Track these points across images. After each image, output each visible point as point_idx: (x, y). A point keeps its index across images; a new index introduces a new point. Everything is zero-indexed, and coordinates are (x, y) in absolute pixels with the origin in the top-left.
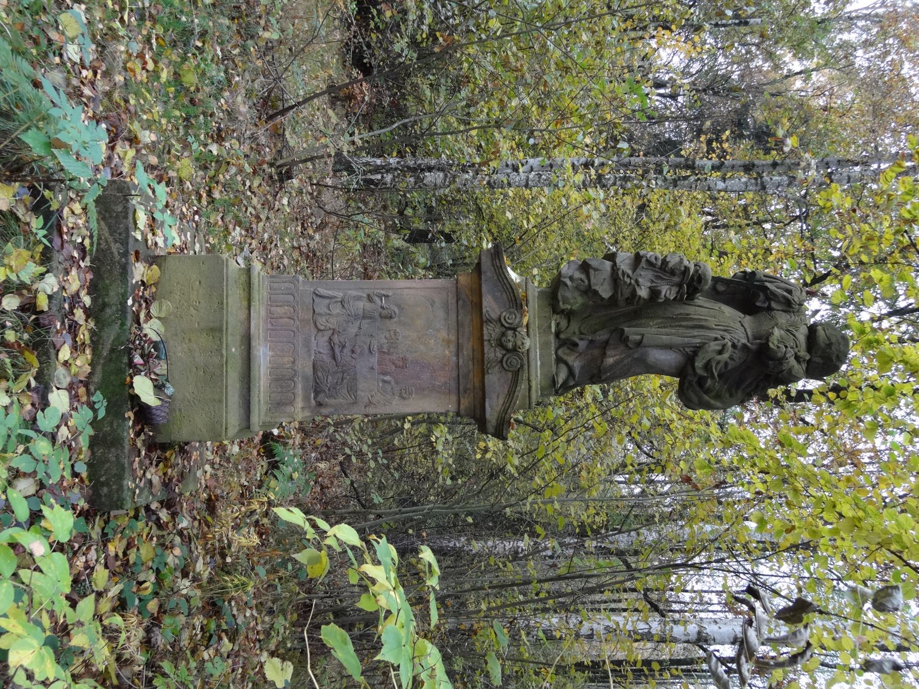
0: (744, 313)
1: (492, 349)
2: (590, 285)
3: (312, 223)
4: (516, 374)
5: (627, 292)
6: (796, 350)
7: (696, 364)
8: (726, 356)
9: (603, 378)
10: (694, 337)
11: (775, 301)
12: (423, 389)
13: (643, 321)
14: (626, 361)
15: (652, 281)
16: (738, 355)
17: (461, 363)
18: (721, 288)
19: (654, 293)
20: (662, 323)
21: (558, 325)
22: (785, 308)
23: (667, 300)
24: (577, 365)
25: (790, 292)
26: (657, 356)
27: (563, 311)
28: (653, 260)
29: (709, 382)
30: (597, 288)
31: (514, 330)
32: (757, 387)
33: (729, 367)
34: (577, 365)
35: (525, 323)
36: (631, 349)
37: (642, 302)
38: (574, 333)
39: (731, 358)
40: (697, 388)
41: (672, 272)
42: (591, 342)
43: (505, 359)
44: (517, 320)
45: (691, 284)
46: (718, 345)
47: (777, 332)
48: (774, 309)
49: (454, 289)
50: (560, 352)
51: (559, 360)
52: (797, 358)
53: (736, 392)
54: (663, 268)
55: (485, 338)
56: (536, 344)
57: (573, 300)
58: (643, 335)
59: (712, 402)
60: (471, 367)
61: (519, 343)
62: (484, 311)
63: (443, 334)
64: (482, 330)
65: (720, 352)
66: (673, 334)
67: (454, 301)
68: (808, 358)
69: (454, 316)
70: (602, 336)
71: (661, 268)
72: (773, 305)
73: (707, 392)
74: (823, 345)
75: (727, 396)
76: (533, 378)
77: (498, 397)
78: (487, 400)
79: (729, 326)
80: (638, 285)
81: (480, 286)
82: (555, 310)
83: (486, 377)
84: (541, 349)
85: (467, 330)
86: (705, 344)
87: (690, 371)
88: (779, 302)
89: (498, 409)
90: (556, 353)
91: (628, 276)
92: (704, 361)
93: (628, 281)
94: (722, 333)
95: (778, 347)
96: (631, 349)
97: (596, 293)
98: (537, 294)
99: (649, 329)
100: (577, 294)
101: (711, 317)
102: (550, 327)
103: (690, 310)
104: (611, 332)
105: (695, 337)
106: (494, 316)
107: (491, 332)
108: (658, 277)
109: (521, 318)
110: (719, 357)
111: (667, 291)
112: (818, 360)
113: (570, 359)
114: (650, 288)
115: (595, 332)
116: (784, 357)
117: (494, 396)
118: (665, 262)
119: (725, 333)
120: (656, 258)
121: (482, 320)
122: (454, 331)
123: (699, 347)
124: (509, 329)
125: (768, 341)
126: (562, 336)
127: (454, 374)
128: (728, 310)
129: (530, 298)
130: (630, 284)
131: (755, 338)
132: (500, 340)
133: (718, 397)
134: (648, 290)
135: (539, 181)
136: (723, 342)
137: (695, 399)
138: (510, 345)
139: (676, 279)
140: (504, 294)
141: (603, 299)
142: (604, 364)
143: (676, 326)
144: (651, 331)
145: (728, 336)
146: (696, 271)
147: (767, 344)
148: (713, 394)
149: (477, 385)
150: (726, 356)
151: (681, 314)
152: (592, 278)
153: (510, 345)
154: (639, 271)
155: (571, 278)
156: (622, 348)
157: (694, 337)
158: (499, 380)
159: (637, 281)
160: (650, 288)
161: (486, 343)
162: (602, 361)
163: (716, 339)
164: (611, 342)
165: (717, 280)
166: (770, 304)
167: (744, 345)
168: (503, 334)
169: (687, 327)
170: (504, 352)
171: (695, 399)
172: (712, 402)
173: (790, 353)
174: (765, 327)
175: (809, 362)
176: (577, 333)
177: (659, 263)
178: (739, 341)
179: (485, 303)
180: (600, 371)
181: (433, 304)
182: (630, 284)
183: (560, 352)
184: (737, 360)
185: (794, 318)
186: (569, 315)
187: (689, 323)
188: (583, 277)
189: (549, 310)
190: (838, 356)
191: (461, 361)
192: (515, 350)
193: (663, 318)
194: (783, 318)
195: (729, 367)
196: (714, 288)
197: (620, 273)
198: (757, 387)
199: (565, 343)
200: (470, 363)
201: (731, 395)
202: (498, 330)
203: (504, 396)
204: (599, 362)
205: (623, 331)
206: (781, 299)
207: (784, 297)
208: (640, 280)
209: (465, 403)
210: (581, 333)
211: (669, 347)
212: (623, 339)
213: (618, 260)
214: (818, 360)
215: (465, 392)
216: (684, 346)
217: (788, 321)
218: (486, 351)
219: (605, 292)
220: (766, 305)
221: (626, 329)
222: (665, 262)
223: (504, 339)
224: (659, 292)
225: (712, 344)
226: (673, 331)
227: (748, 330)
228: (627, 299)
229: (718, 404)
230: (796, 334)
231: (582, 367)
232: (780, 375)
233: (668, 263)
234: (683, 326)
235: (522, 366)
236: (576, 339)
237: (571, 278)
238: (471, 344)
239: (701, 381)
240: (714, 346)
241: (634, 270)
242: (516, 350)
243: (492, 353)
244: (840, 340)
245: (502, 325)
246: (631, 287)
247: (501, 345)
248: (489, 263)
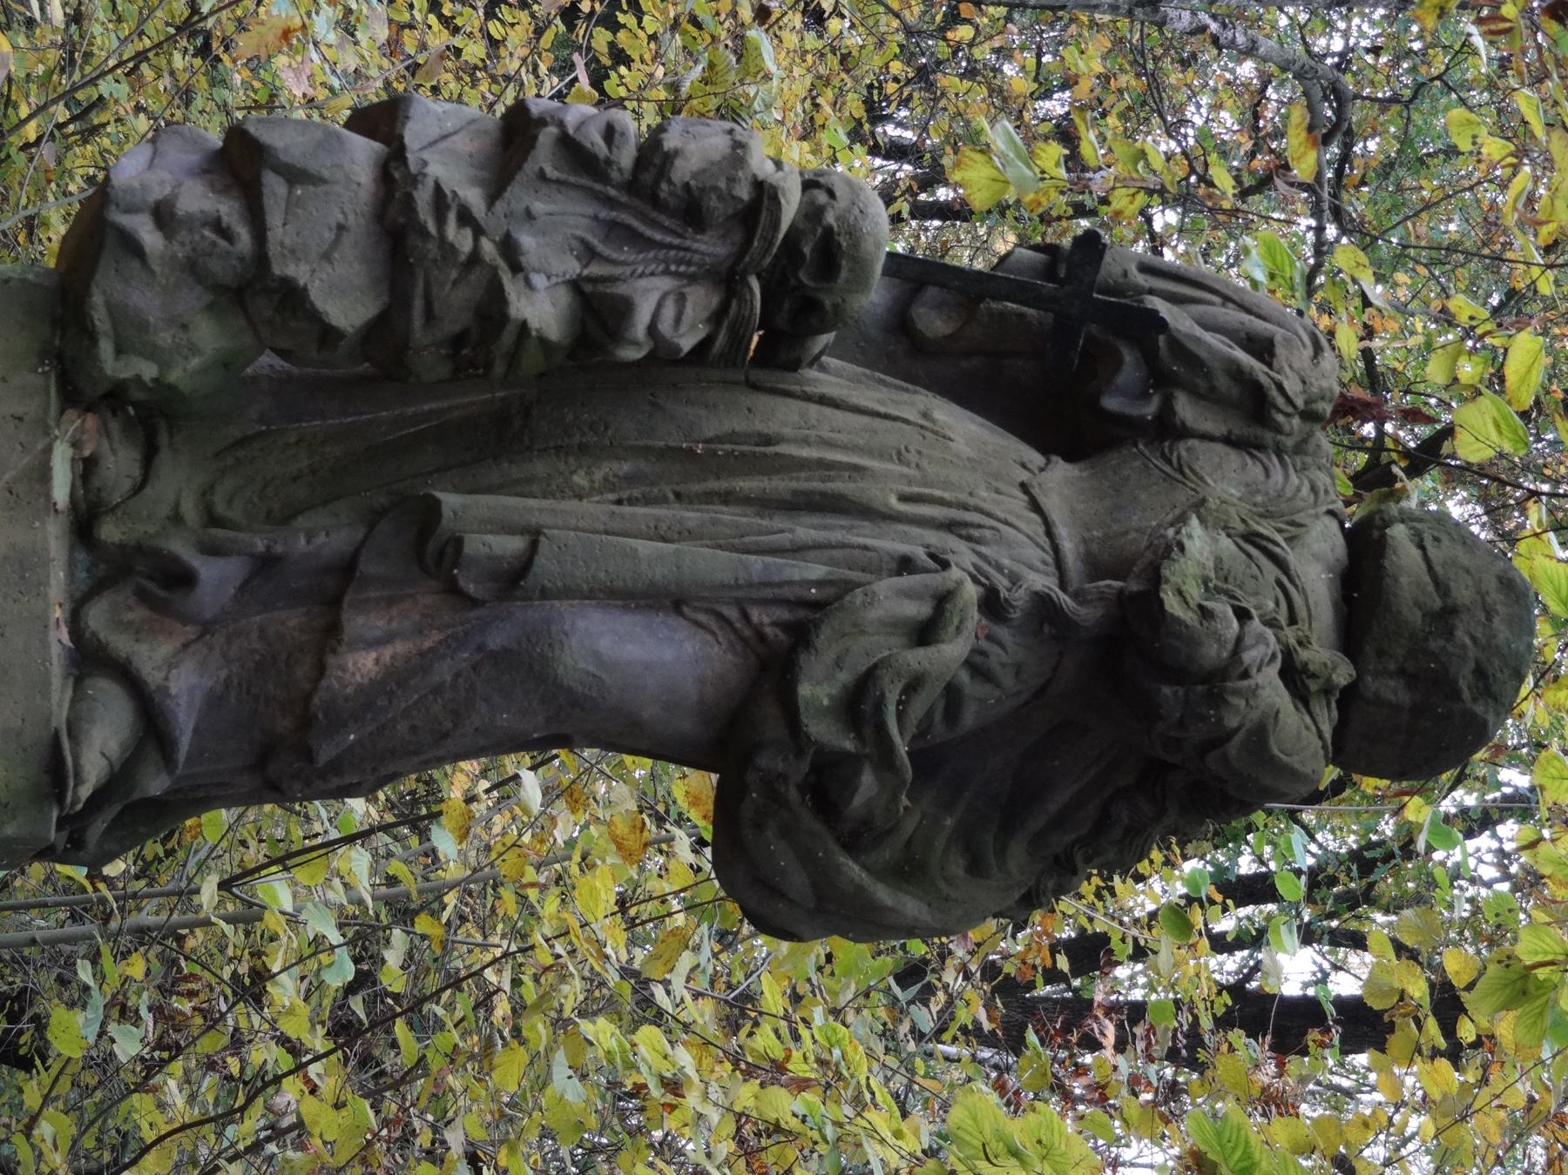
0: (1045, 449)
2: (261, 257)
5: (457, 302)
6: (1290, 635)
7: (805, 690)
8: (952, 651)
9: (326, 753)
10: (797, 550)
11: (1195, 394)
13: (540, 467)
14: (443, 671)
15: (589, 253)
16: (1009, 650)
18: (933, 322)
19: (597, 311)
20: (630, 479)
21: (87, 468)
22: (1240, 429)
23: (662, 356)
24: (184, 679)
25: (1263, 348)
26: (605, 645)
27: (114, 398)
28: (594, 139)
29: (868, 782)
30: (299, 272)
32: (1102, 823)
33: (970, 717)
34: (184, 679)
36: (474, 603)
37: (532, 360)
38: (176, 518)
39: (976, 666)
40: (809, 821)
41: (691, 211)
42: (266, 564)
45: (784, 280)
46: (909, 594)
47: (1201, 545)
48: (1184, 433)
50: (96, 617)
51: (89, 659)
52: (1293, 674)
53: (1001, 853)
54: (646, 194)
57: (172, 335)
58: (534, 535)
59: (883, 894)
65: (925, 633)
66: (690, 535)
68: (1343, 674)
70: (322, 537)
71: (632, 186)
72: (1186, 409)
73: (854, 843)
74: (1415, 618)
75: (957, 867)
79: (964, 510)
80: (516, 268)
82: (76, 388)
86: (848, 586)
87: (772, 725)
88: (1207, 396)
90: (75, 622)
91: (466, 218)
92: (845, 677)
93: (463, 241)
94: (933, 538)
95: (1205, 613)
96: (474, 603)
97: (292, 297)
99: (571, 505)
100: (191, 300)
101: (882, 455)
102: (43, 474)
103: (780, 416)
104: (373, 518)
105: (803, 554)
108: (616, 232)
110: (918, 658)
111: (664, 306)
112: (1392, 690)
113: (151, 657)
114: (575, 285)
115: (283, 518)
116: (1233, 668)
118: (653, 153)
119: (951, 542)
120: (610, 133)
123: (818, 605)
125: (1155, 579)
126: (110, 531)
128: (964, 428)
130: (475, 257)
131: (1096, 568)
133: (909, 871)
134: (564, 296)
136: (937, 580)
137: (798, 881)
139: (711, 247)
141: (328, 334)
142: (331, 681)
143: (709, 497)
144: (577, 517)
145: (962, 554)
146: (812, 213)
147: (1149, 600)
148: (887, 854)
150: (952, 651)
151: (733, 437)
152: (274, 219)
154: (519, 195)
155: (163, 215)
156: (428, 598)
157: (797, 550)
159: (509, 248)
160: (575, 285)
162: (321, 669)
163: (905, 565)
164: (368, 567)
165: (914, 274)
166: (1167, 408)
167: (1043, 604)
169: (767, 504)
171: (798, 881)
172: (883, 894)
173: (1262, 648)
174: (1145, 517)
175: (1348, 698)
176: (190, 510)
177: (626, 157)
178: (1015, 579)
180: (306, 721)
182: (475, 257)
183: (96, 617)
184: (1008, 679)
185: (1280, 478)
186: (149, 417)
187: (779, 485)
188: (228, 210)
190: (1480, 672)
193: (646, 452)
194: (1227, 477)
195: (970, 717)
196: (900, 323)
197: (423, 198)
198: (1102, 823)
199: (126, 569)
201: (976, 867)
204: (303, 671)
205: (433, 508)
206: (1222, 382)
207: (1237, 373)
208: (527, 241)
210: (213, 520)
211: (669, 600)
212: (433, 554)
213: (414, 134)
214: (1392, 690)
216: (745, 595)
217: (1251, 489)
219: (344, 299)
220: (1150, 409)
221: (450, 501)
222: (653, 153)
224: (624, 308)
225: (885, 586)
226: (692, 517)
227: (1063, 532)
228: (458, 340)
229: (912, 907)
230: (1291, 557)
231: (214, 701)
232: (1212, 758)
233: (670, 157)
234: (746, 500)
236: (181, 548)
237: (163, 215)
239: (826, 782)
240: (895, 600)
241: (495, 192)
244: (1495, 596)
246: (475, 276)
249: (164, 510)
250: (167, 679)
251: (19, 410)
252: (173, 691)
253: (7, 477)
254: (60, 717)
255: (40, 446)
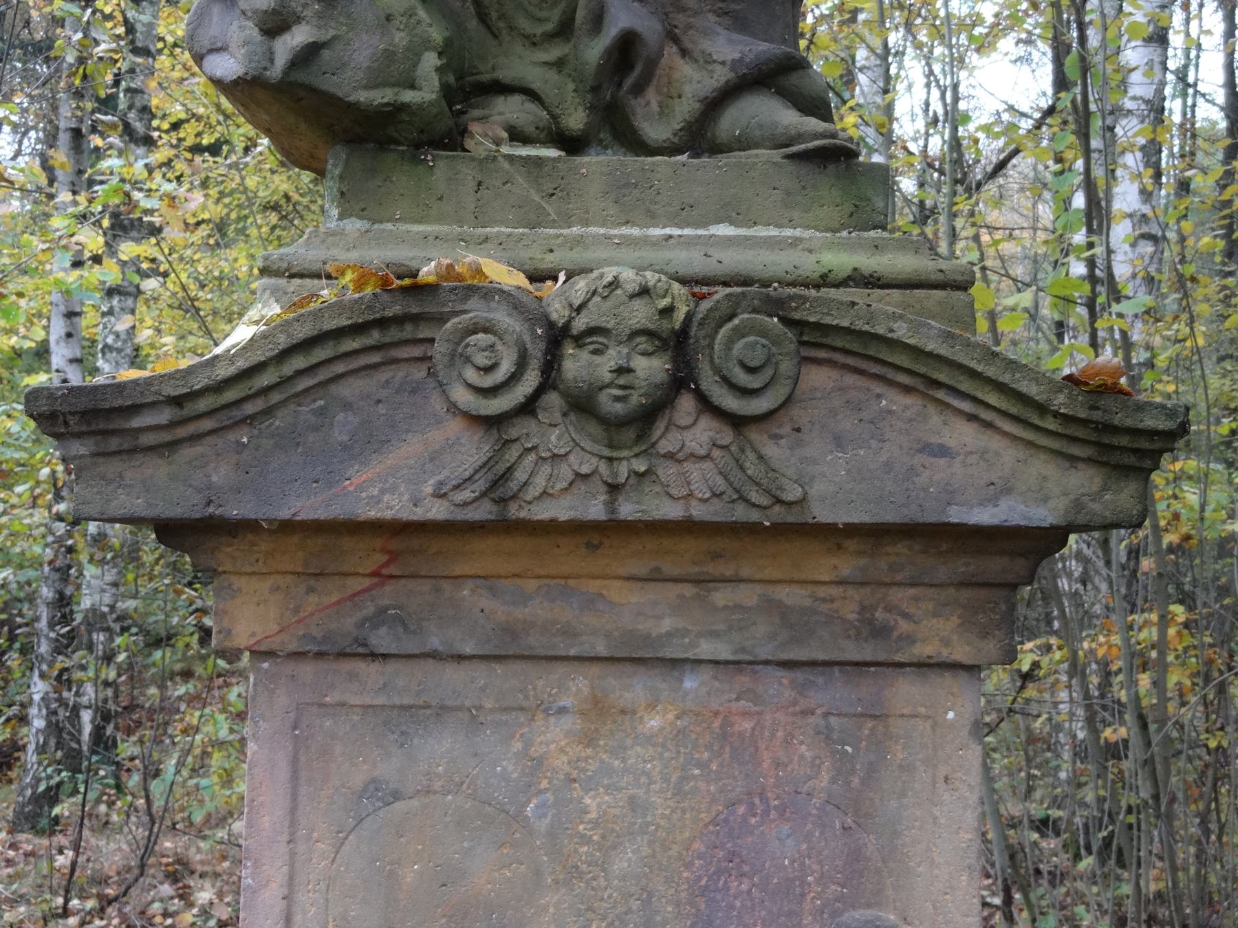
1: (667, 472)
3: (166, 914)
4: (816, 339)
12: (856, 855)
17: (723, 651)
21: (517, 136)
31: (558, 337)
35: (521, 280)
38: (559, 64)
43: (731, 403)
44: (503, 317)
49: (307, 670)
50: (656, 132)
51: (699, 138)
55: (596, 510)
56: (631, 245)
60: (748, 595)
61: (640, 314)
62: (437, 511)
63: (554, 737)
64: (551, 528)
67: (371, 671)
69: (453, 675)
76: (809, 265)
77: (942, 451)
78: (955, 515)
81: (288, 527)
83: (823, 514)
84: (652, 218)
85: (538, 610)
89: (1009, 455)
98: (354, 225)
106: (471, 451)
107: (562, 476)
109: (489, 292)
113: (692, 82)
117: (937, 472)
121: (497, 526)
122: (543, 681)
124: (551, 366)
126: (576, 120)
127: (778, 685)
129: (378, 256)
132: (612, 425)
135: (119, 351)
138: (651, 368)
140: (348, 390)
149: (847, 566)
153: (651, 368)
158: (839, 442)
161: (627, 510)
168: (582, 404)
170: (686, 404)
179: (395, 506)
181: (381, 794)
189: (441, 166)
191: (706, 649)
192: (677, 343)
200: (722, 596)
202: (553, 432)
203: (935, 418)
209: (937, 632)
210: (565, 30)
215: (880, 632)
218: (673, 511)
223: (607, 403)
235: (774, 306)
236: (594, 50)
238: (617, 592)
242: (682, 336)
243: (690, 472)
245: (528, 408)
247: (649, 417)
248: (156, 470)
249: (552, 75)
250: (723, 63)
251: (472, 184)
252: (737, 56)
253: (537, 199)
254: (776, 155)
255: (506, 165)
